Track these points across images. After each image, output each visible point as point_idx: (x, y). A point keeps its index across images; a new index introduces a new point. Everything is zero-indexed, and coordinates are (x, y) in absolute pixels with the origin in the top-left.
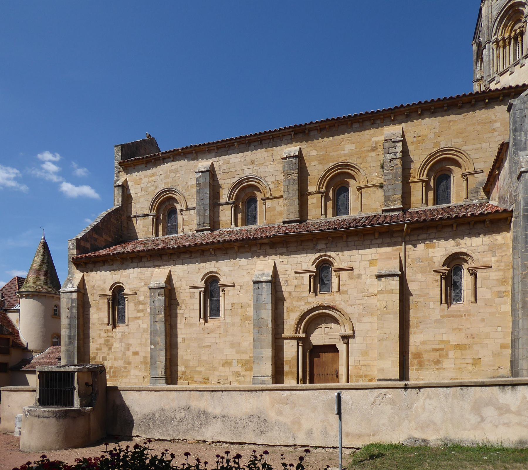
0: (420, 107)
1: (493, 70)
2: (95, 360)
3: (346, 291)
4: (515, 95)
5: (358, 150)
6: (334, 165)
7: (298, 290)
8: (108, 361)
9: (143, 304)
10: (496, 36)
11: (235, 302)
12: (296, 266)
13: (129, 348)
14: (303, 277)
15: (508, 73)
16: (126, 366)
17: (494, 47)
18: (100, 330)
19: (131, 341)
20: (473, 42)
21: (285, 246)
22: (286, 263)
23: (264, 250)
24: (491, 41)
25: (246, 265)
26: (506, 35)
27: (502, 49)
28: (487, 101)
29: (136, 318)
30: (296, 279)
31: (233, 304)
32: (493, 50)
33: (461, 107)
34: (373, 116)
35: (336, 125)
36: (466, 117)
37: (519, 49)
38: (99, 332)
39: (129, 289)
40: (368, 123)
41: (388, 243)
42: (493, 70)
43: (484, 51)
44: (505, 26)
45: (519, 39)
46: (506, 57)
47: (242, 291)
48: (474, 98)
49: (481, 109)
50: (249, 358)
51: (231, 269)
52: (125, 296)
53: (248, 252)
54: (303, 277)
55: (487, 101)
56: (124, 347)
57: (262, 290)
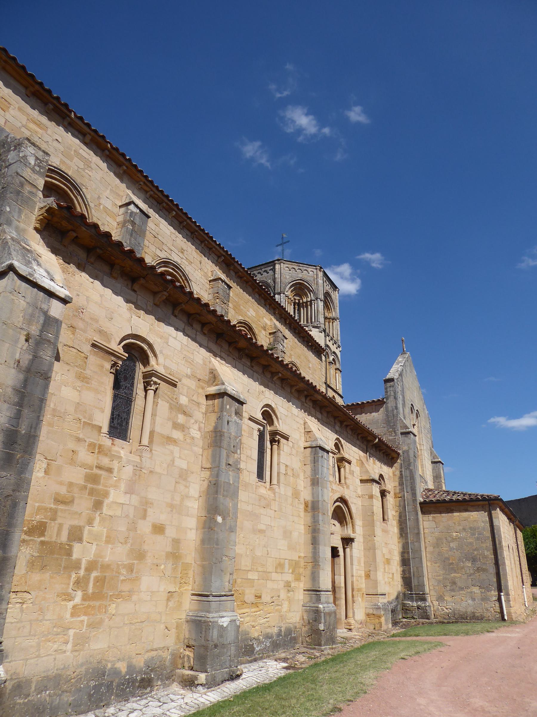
0: (289, 318)
2: (42, 534)
8: (85, 543)
9: (185, 413)
13: (145, 511)
16: (133, 564)
18: (79, 440)
19: (153, 494)
29: (170, 440)
31: (287, 466)
34: (269, 300)
35: (250, 283)
38: (72, 445)
39: (165, 367)
52: (154, 379)
56: (135, 507)
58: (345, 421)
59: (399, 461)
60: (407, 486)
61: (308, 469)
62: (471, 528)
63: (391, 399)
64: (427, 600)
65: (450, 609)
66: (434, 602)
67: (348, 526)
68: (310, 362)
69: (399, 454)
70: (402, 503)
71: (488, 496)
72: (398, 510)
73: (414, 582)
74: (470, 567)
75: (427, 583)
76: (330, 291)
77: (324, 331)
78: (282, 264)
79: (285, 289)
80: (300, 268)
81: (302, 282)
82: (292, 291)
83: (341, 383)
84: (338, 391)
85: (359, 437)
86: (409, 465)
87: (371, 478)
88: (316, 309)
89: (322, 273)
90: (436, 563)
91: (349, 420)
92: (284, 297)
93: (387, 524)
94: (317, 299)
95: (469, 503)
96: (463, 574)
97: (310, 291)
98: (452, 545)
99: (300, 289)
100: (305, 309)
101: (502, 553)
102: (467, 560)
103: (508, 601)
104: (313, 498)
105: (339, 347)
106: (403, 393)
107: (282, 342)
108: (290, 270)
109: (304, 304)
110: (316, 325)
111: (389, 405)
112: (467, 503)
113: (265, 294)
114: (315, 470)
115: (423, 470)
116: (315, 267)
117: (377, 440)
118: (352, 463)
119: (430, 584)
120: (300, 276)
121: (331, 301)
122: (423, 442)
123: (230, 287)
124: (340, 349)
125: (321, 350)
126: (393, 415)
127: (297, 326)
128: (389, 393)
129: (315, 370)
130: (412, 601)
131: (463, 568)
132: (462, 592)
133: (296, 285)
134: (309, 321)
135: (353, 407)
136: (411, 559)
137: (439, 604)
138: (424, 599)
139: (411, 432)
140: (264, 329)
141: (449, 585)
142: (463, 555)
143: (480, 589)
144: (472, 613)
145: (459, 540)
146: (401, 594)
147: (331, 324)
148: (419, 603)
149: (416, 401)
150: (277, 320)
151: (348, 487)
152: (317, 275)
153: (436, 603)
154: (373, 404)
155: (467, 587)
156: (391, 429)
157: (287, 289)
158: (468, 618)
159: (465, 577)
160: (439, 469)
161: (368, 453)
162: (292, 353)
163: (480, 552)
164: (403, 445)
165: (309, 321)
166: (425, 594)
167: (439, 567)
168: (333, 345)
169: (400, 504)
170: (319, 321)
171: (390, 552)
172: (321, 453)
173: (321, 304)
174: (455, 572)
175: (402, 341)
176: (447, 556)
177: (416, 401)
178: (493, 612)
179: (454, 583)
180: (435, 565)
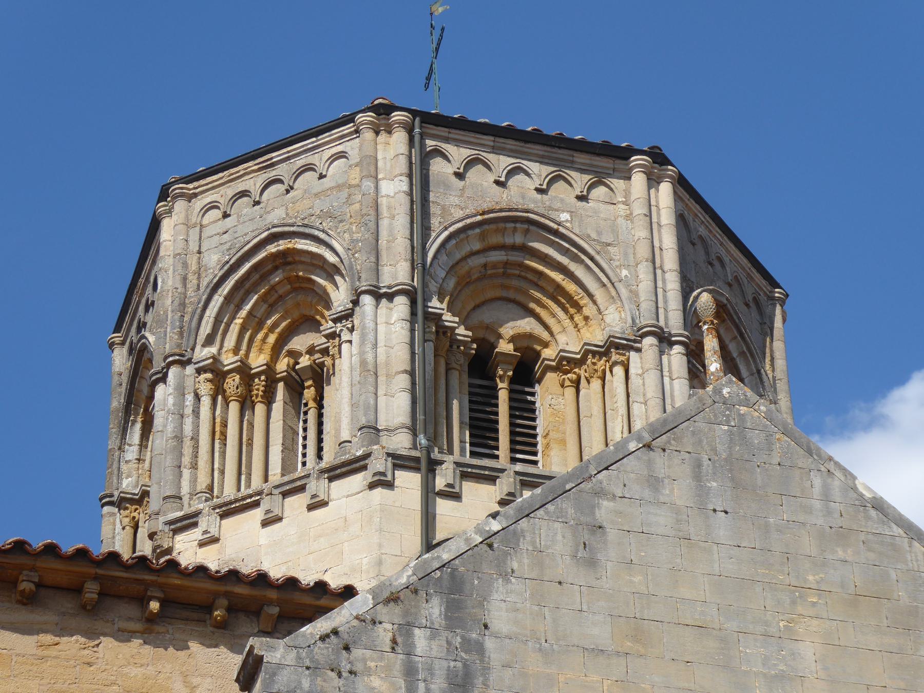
1: (194, 480)
4: (282, 617)
10: (213, 350)
15: (257, 514)
17: (205, 389)
20: (117, 337)
24: (189, 362)
26: (258, 361)
27: (234, 407)
28: (154, 606)
32: (197, 397)
33: (29, 600)
36: (53, 652)
37: (305, 430)
42: (194, 480)
43: (160, 391)
44: (254, 323)
45: (309, 394)
46: (250, 444)
48: (96, 578)
49: (124, 636)
55: (154, 606)
81: (283, 245)
82: (254, 323)
94: (356, 303)
97: (331, 271)
108: (226, 215)
121: (565, 252)
133: (264, 278)
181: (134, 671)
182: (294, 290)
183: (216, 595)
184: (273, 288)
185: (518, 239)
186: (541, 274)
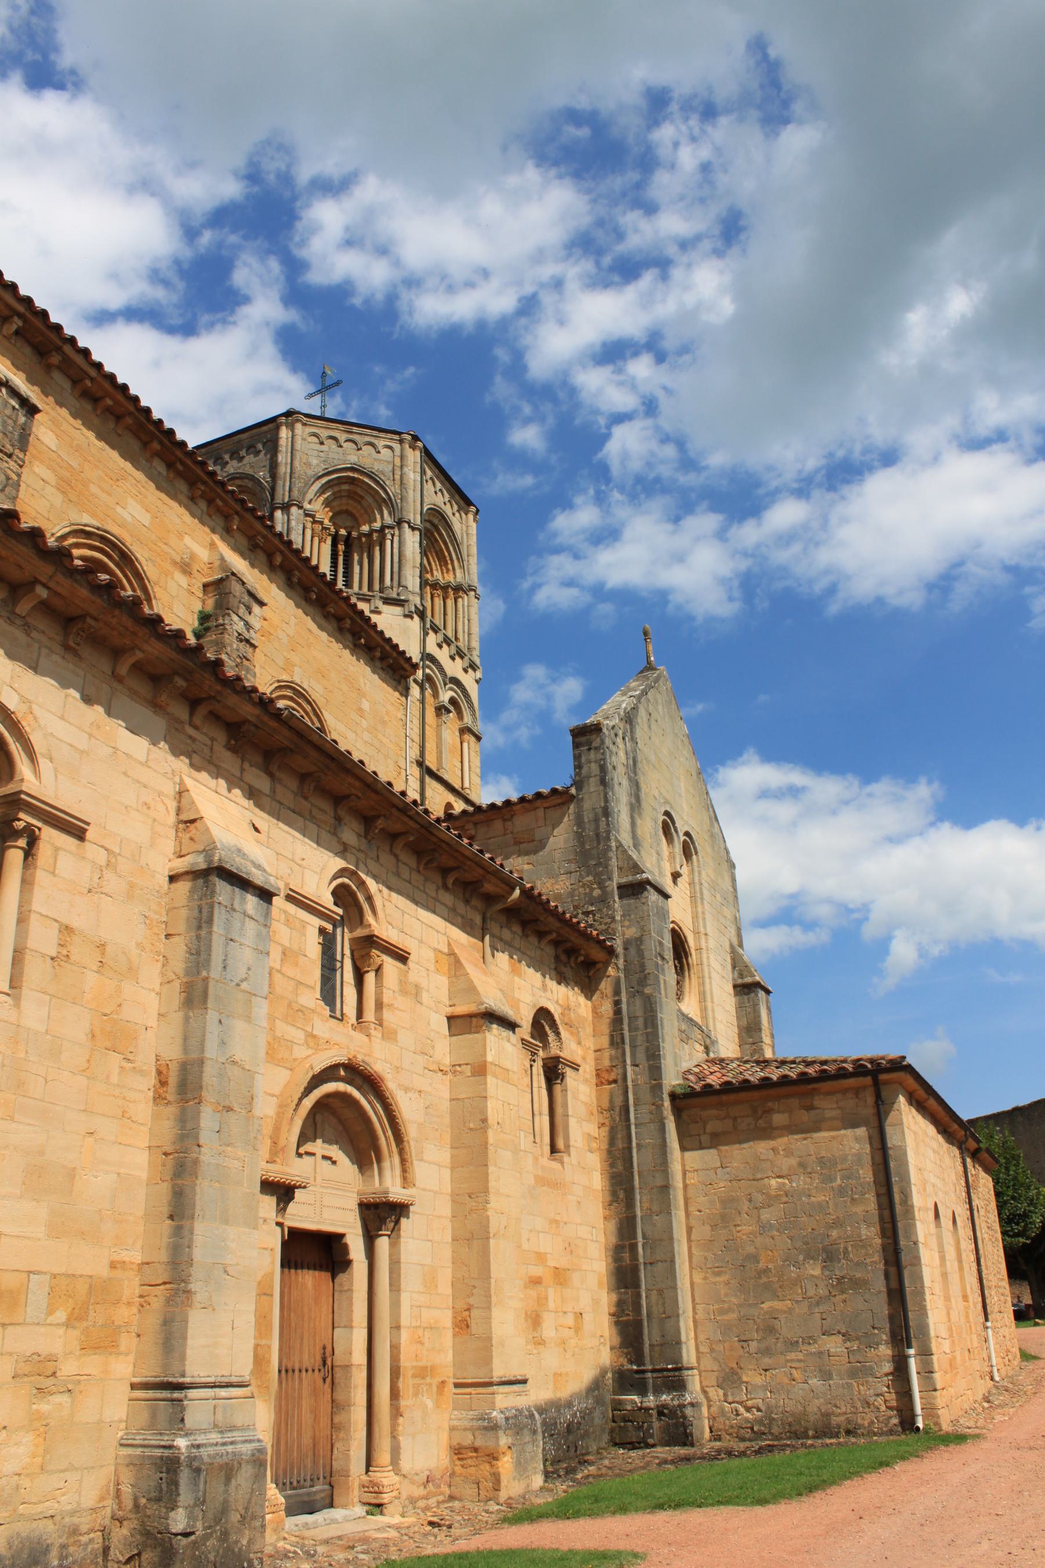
0: (282, 552)
3: (395, 1032)
5: (154, 537)
6: (98, 529)
7: (289, 971)
11: (75, 923)
12: (289, 871)
14: (304, 924)
21: (274, 768)
22: (262, 837)
23: (209, 742)
25: (141, 763)
30: (287, 922)
31: (67, 929)
33: (327, 616)
34: (204, 483)
40: (182, 486)
41: (462, 917)
47: (113, 883)
48: (351, 618)
50: (105, 1272)
51: (83, 743)
53: (156, 706)
54: (304, 924)
55: (363, 641)
57: (243, 924)
58: (379, 816)
59: (611, 971)
60: (633, 1047)
61: (178, 949)
62: (821, 1161)
63: (593, 786)
64: (690, 1386)
65: (759, 1410)
66: (712, 1393)
67: (386, 1164)
68: (364, 695)
69: (611, 952)
70: (619, 1101)
71: (872, 1061)
72: (607, 1122)
73: (650, 1336)
74: (816, 1277)
75: (692, 1335)
76: (448, 510)
77: (422, 615)
78: (299, 426)
79: (305, 494)
80: (351, 437)
83: (478, 771)
84: (468, 791)
85: (450, 882)
86: (643, 981)
87: (482, 1008)
88: (396, 551)
89: (418, 453)
90: (718, 1274)
91: (394, 810)
92: (302, 517)
93: (562, 1163)
94: (399, 523)
95: (816, 1086)
96: (797, 1302)
98: (766, 1215)
99: (352, 495)
100: (365, 555)
101: (911, 1227)
102: (809, 1256)
103: (927, 1372)
104: (185, 1049)
105: (473, 666)
106: (635, 773)
107: (242, 610)
108: (322, 443)
109: (364, 539)
110: (394, 596)
111: (587, 805)
112: (811, 1086)
113: (189, 462)
114: (198, 953)
115: (706, 1009)
116: (397, 437)
117: (517, 892)
118: (411, 958)
119: (702, 1337)
120: (353, 458)
121: (449, 537)
122: (705, 927)
123: (32, 410)
124: (479, 674)
125: (402, 662)
126: (598, 835)
127: (313, 577)
128: (584, 771)
129: (384, 723)
130: (643, 1392)
131: (797, 1281)
132: (792, 1356)
133: (339, 484)
134: (377, 587)
135: (481, 817)
136: (642, 1267)
137: (725, 1395)
138: (678, 1385)
139: (648, 882)
140: (186, 568)
141: (756, 1336)
142: (799, 1244)
143: (845, 1342)
144: (823, 1415)
145: (784, 1199)
146: (610, 1375)
147: (450, 603)
148: (664, 1397)
149: (685, 806)
150: (243, 555)
151: (390, 1036)
152: (402, 457)
153: (716, 1394)
154: (539, 803)
155: (809, 1340)
156: (590, 878)
157: (310, 495)
158: (811, 1433)
159: (803, 1308)
160: (755, 1007)
161: (487, 938)
162: (295, 658)
163: (846, 1231)
164: (627, 923)
165: (377, 587)
166: (679, 1369)
167: (727, 1283)
168: (452, 658)
169: (611, 1101)
170: (403, 583)
171: (569, 1248)
172: (223, 890)
173: (412, 541)
174: (776, 1296)
175: (646, 633)
176: (751, 1249)
177: (685, 806)
178: (883, 1408)
179: (771, 1330)
180: (718, 1279)
181: (351, 668)
182: (349, 497)
183: (378, 645)
184: (340, 491)
185: (436, 521)
186: (437, 541)
